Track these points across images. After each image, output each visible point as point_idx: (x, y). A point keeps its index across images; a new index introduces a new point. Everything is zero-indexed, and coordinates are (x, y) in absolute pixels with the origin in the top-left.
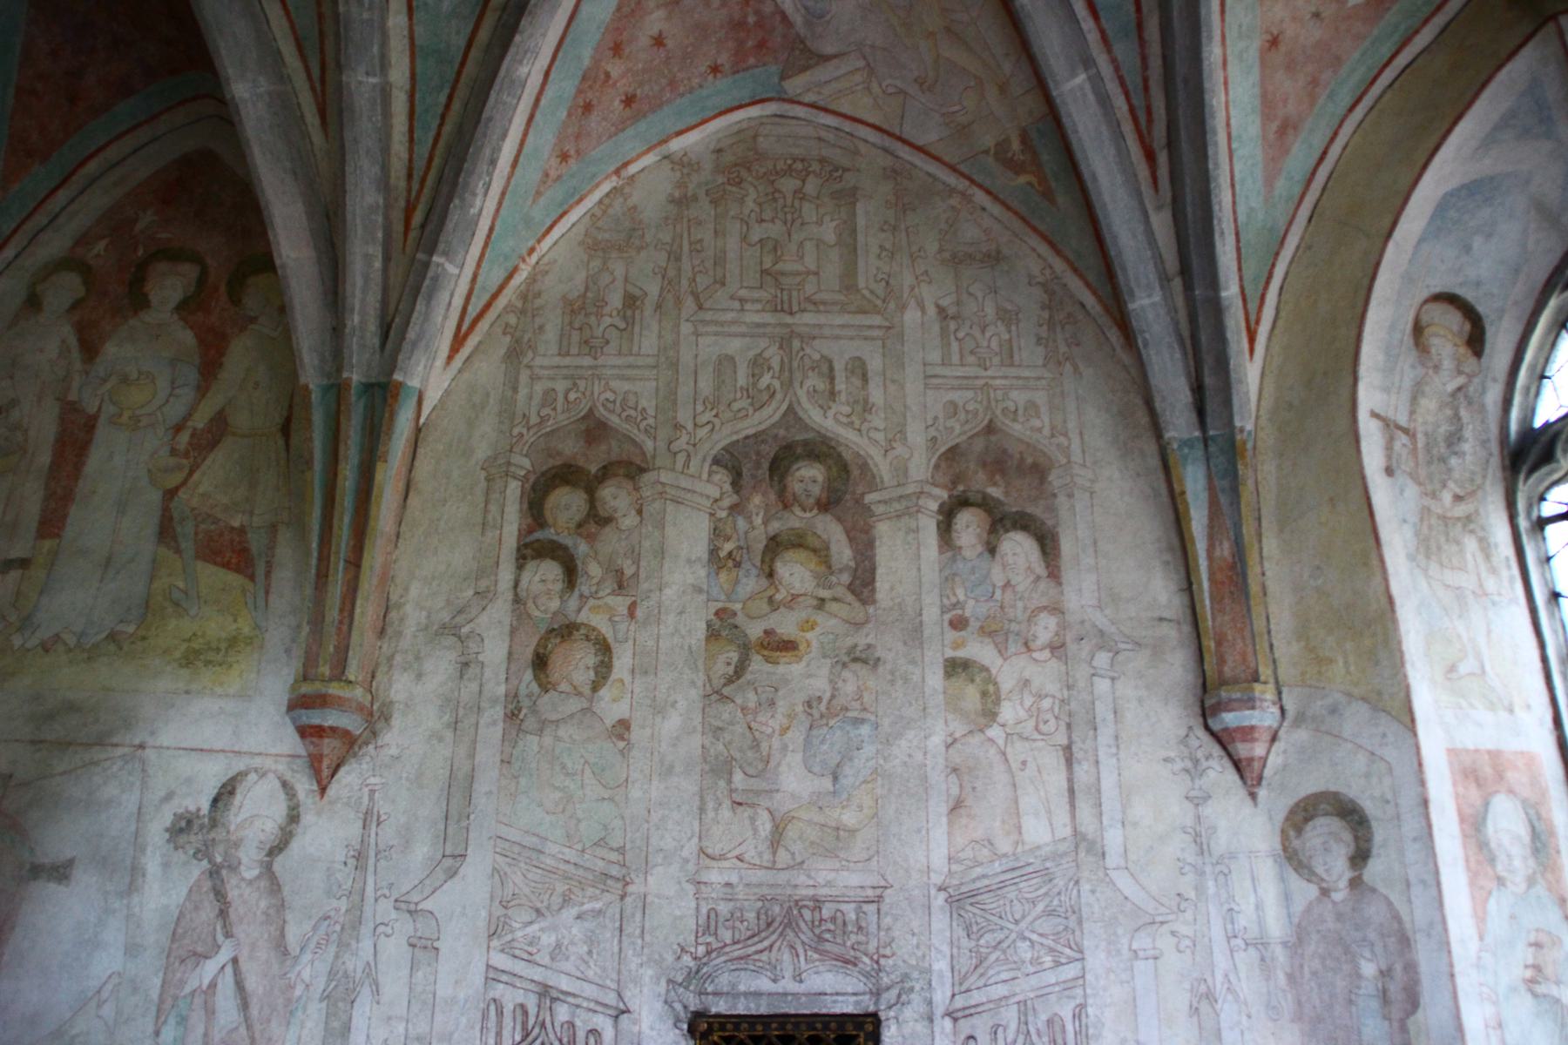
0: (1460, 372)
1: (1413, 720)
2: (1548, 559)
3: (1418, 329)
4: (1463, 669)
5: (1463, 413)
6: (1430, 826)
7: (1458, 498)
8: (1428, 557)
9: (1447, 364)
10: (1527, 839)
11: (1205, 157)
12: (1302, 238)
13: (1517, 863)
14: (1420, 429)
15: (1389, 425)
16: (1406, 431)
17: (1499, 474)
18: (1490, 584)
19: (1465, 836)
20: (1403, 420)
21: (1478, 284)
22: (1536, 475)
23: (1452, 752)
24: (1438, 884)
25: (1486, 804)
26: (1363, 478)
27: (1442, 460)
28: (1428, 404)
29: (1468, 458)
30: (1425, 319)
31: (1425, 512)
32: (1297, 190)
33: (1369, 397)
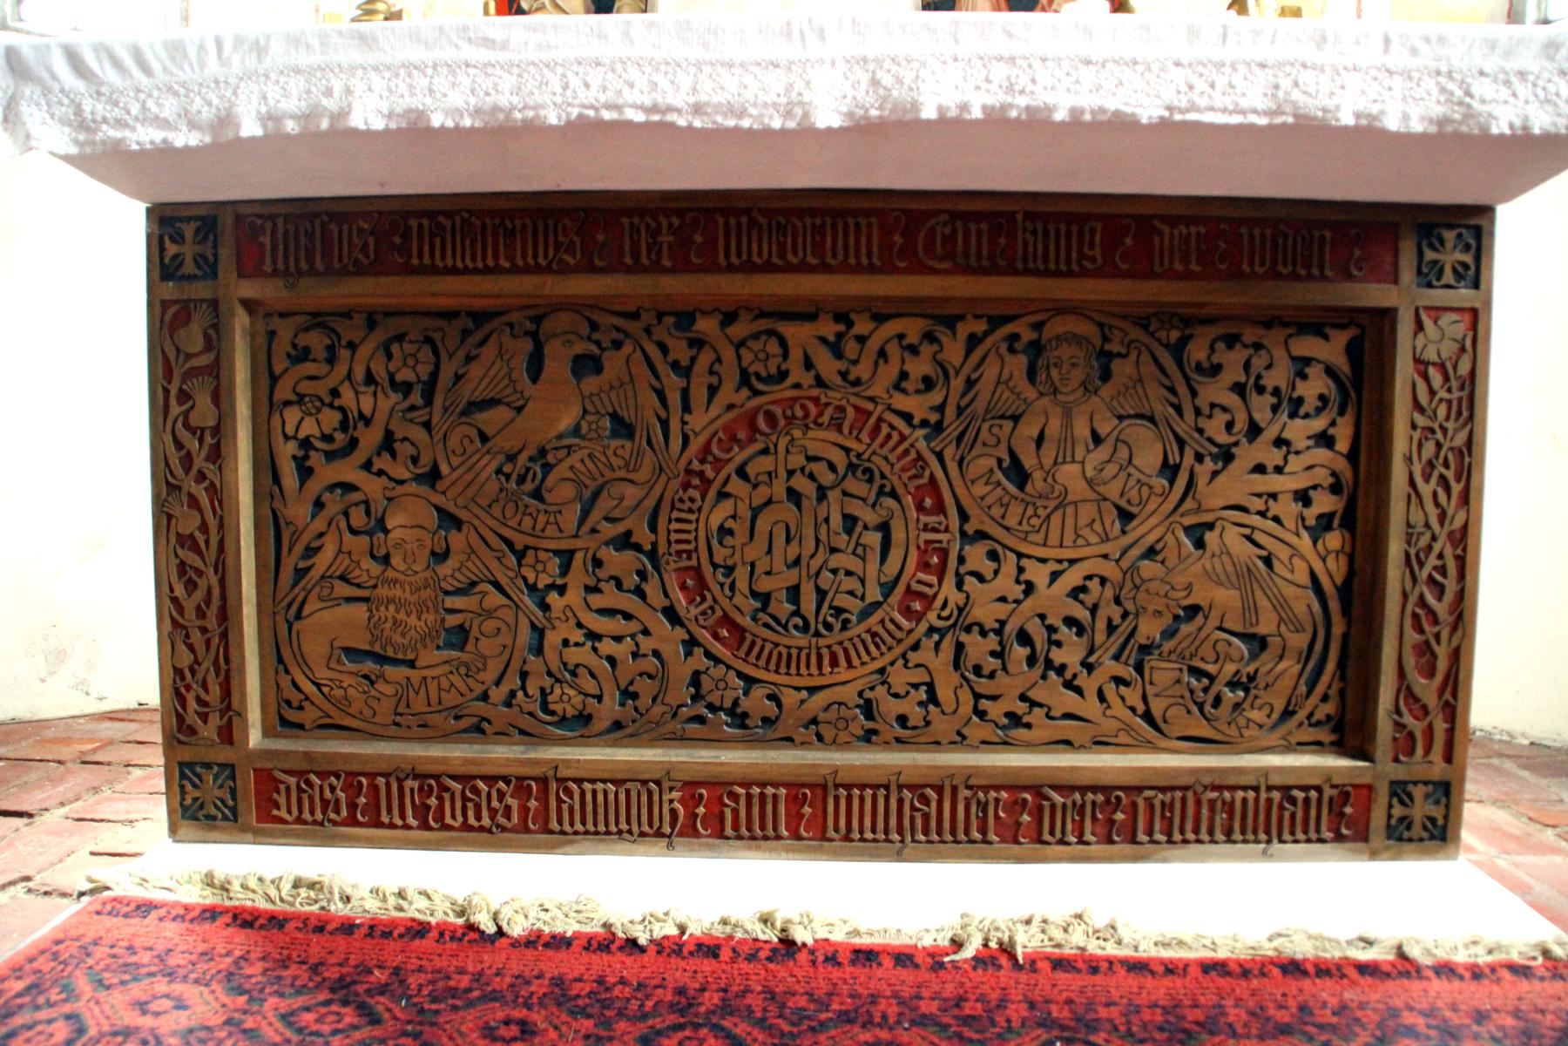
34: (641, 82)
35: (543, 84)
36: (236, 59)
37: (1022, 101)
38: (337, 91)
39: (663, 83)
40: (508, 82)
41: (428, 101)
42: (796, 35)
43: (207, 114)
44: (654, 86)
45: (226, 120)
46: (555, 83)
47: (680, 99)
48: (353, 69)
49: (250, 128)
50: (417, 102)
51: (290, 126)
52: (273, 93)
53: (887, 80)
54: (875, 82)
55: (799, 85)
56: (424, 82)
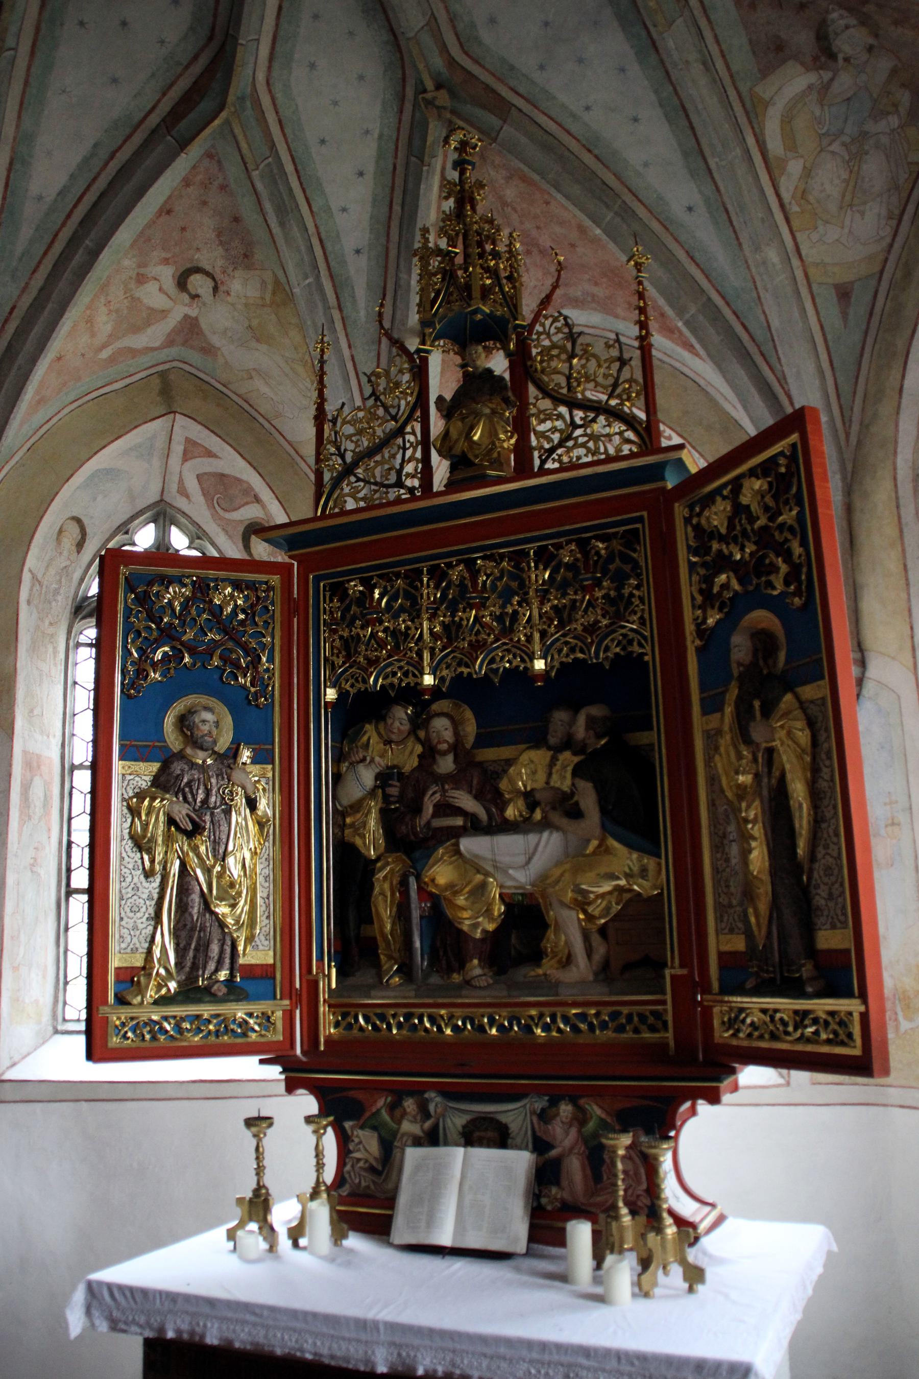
0: (69, 559)
1: (13, 733)
2: (76, 664)
3: (60, 531)
4: (36, 712)
5: (63, 580)
6: (10, 787)
7: (51, 624)
8: (33, 651)
9: (65, 553)
10: (42, 799)
11: (11, 412)
12: (21, 458)
13: (37, 810)
14: (45, 583)
15: (34, 577)
16: (40, 583)
17: (68, 615)
18: (53, 672)
19: (22, 794)
20: (40, 576)
21: (92, 517)
22: (83, 621)
23: (25, 752)
24: (8, 815)
25: (32, 780)
26: (18, 603)
27: (50, 603)
28: (52, 571)
29: (59, 604)
30: (65, 527)
31: (37, 628)
32: (31, 433)
33: (31, 561)
34: (310, 1341)
35: (275, 1336)
36: (166, 1304)
37: (458, 1372)
38: (201, 1324)
39: (319, 1343)
40: (262, 1332)
41: (233, 1336)
42: (369, 1329)
43: (155, 1325)
44: (315, 1344)
45: (162, 1330)
46: (279, 1335)
47: (325, 1351)
48: (207, 1317)
49: (170, 1334)
50: (231, 1335)
51: (186, 1336)
52: (179, 1322)
53: (404, 1354)
54: (399, 1355)
55: (370, 1352)
56: (232, 1327)
